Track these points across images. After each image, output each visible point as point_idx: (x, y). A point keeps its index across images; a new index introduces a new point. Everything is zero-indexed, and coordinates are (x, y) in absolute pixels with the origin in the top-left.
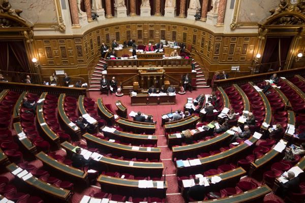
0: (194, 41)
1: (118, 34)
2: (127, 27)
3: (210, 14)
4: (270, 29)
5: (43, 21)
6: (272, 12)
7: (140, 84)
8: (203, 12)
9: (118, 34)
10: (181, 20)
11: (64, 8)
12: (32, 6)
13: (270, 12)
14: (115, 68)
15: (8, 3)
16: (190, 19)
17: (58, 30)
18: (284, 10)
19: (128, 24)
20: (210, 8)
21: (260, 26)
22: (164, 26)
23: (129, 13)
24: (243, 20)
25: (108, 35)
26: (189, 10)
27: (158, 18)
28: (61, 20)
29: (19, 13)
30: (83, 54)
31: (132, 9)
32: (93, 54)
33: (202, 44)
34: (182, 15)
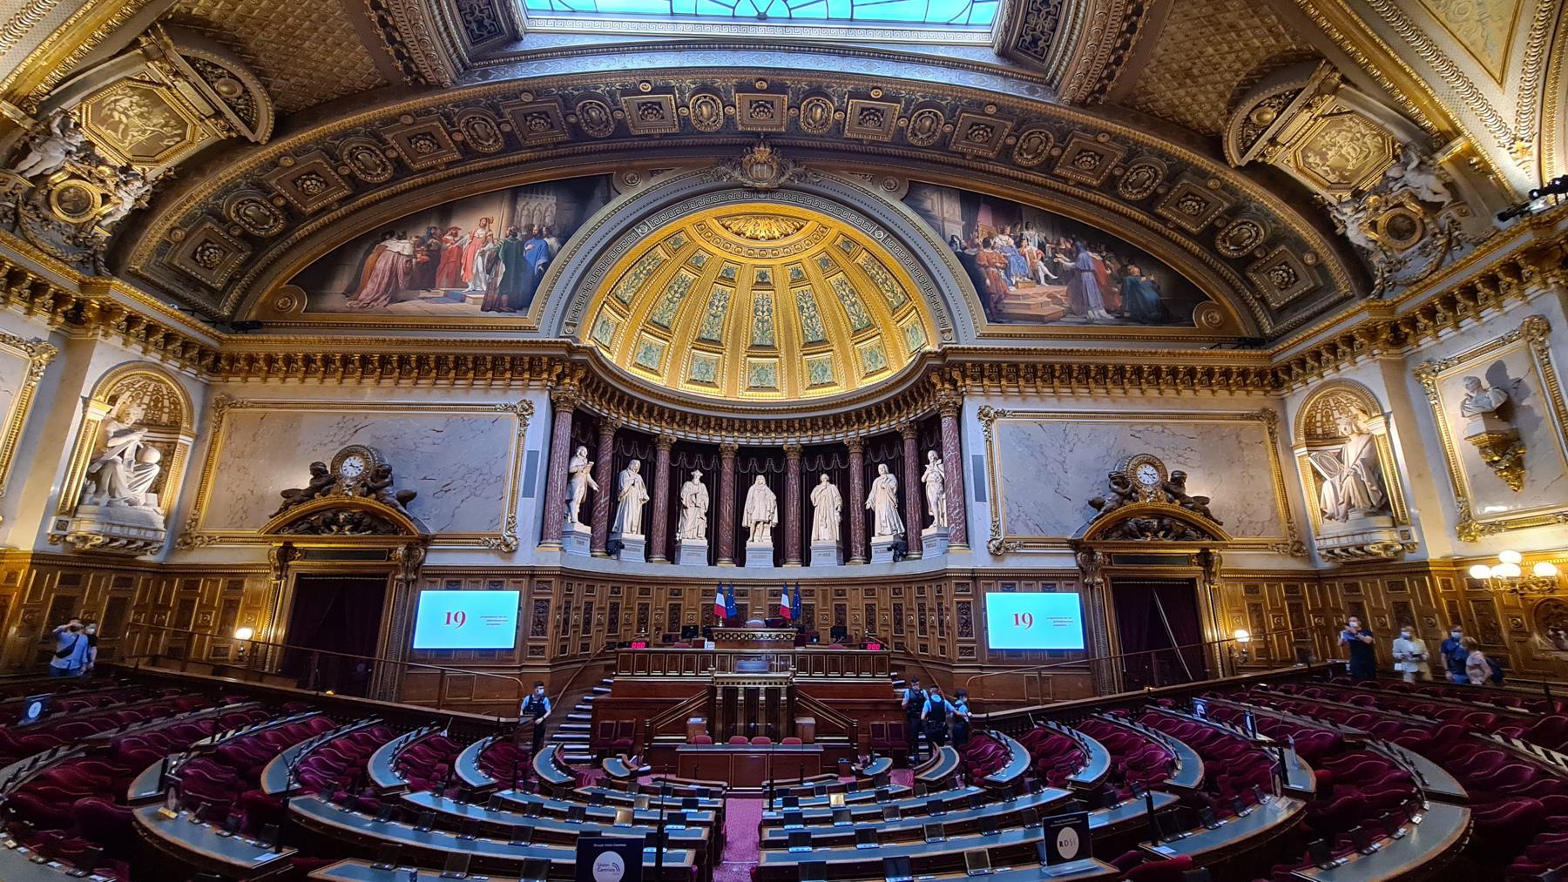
0: (899, 622)
1: (675, 609)
2: (705, 593)
3: (925, 532)
4: (1109, 555)
5: (462, 528)
6: (1096, 504)
7: (710, 727)
8: (911, 536)
9: (675, 609)
10: (856, 569)
11: (528, 493)
12: (446, 489)
13: (1092, 503)
14: (642, 677)
15: (389, 471)
16: (882, 564)
17: (498, 550)
18: (1129, 497)
19: (708, 588)
20: (926, 521)
21: (1076, 545)
22: (811, 593)
23: (713, 559)
24: (1022, 533)
25: (644, 608)
26: (874, 540)
27: (792, 571)
28: (511, 525)
29: (406, 498)
30: (550, 628)
31: (724, 549)
32: (585, 647)
33: (922, 623)
34: (858, 558)
